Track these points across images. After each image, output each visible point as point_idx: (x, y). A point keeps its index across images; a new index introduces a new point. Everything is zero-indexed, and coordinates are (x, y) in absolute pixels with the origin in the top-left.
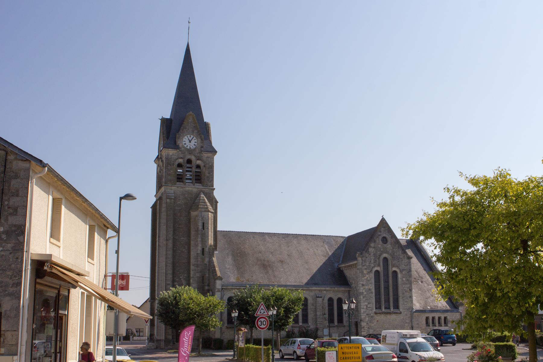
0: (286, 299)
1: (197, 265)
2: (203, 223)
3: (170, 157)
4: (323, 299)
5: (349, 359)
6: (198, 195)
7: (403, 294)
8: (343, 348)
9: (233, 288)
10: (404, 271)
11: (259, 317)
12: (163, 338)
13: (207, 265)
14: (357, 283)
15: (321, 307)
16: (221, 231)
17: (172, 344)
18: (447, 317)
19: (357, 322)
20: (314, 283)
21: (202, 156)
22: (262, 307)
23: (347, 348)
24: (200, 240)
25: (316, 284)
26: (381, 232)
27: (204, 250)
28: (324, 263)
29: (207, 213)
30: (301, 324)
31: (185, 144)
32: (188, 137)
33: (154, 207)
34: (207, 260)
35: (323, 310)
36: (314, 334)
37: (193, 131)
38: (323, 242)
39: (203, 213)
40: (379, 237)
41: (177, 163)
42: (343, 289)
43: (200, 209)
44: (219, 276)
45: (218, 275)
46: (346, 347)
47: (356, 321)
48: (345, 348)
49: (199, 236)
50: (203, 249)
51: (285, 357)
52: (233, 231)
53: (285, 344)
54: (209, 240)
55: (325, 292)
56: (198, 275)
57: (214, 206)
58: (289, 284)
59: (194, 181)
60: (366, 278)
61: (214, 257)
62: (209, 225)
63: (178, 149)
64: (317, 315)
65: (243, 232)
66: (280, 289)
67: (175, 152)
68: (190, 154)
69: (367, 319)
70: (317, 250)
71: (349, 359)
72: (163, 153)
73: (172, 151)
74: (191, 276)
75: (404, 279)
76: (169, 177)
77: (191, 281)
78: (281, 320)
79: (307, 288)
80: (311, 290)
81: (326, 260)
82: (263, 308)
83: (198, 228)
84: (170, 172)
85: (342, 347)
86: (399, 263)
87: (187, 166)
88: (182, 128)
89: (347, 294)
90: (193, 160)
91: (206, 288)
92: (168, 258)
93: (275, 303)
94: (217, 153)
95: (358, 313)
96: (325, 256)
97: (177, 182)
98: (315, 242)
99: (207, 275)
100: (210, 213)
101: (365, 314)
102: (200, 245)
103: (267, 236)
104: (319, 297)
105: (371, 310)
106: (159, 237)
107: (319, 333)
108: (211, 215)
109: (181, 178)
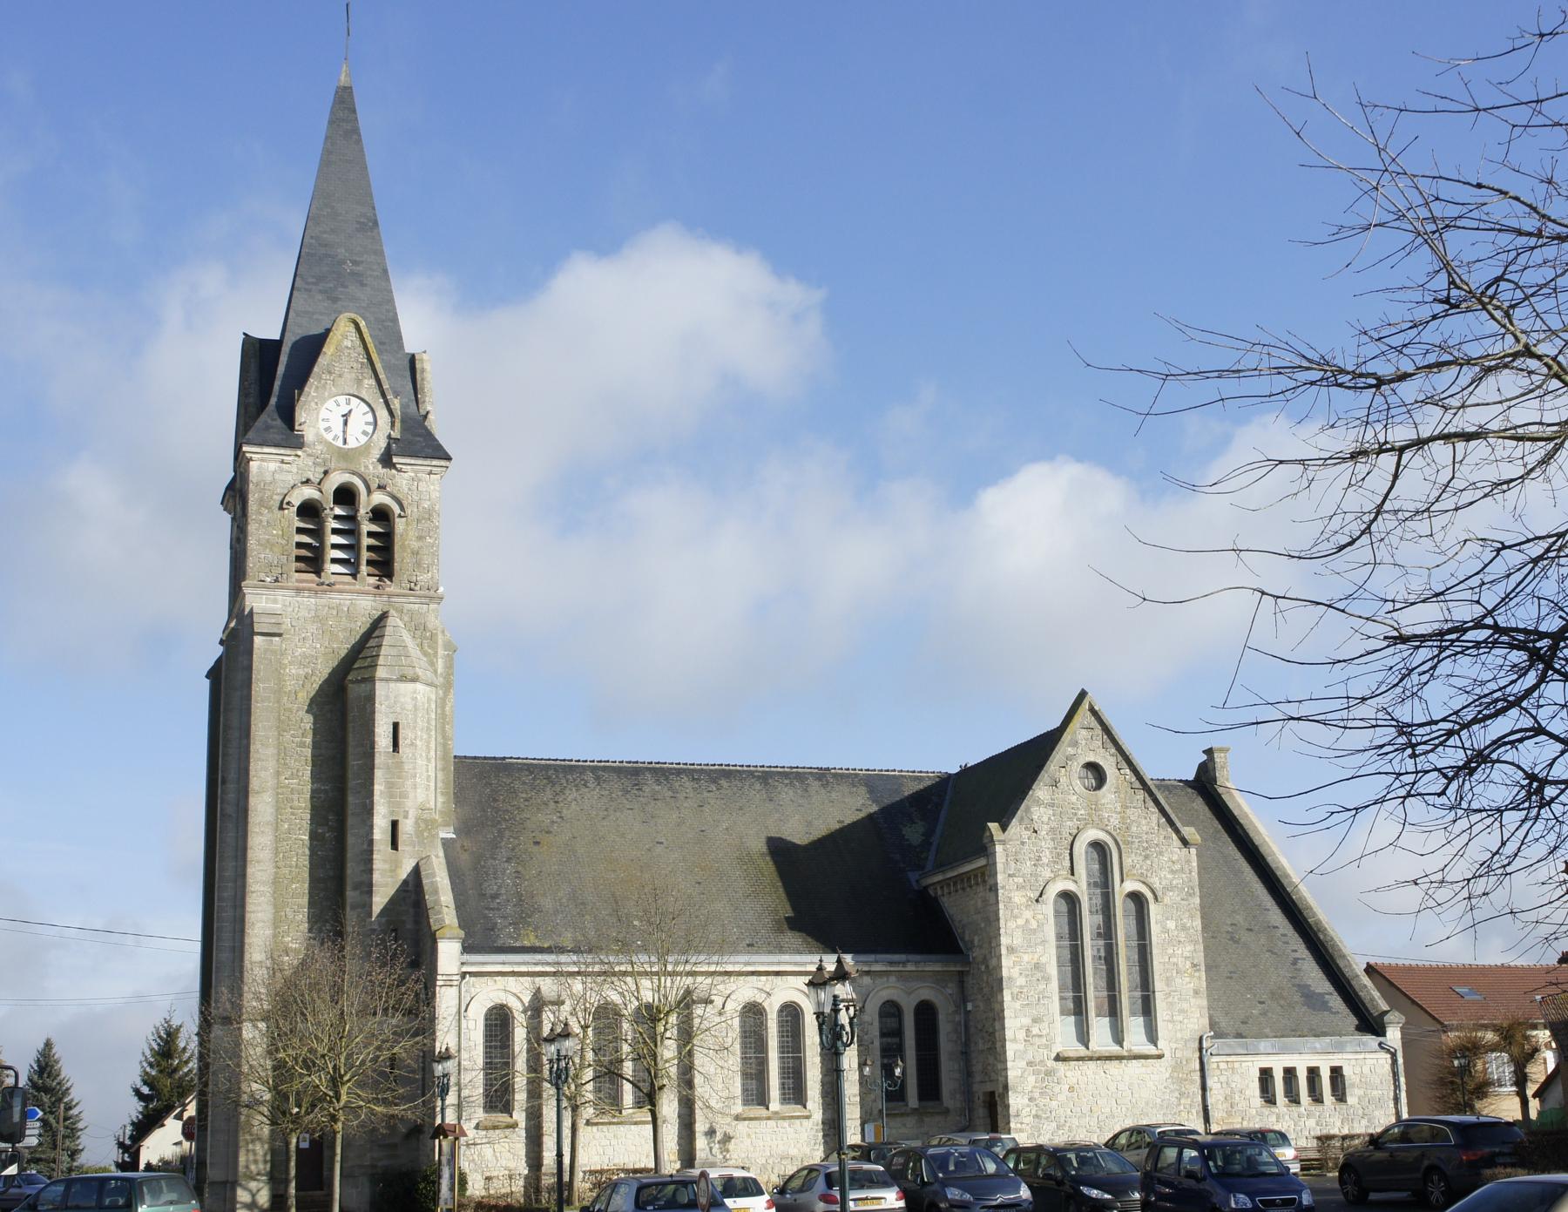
3: (269, 479)
7: (1168, 981)
10: (1171, 894)
14: (990, 943)
18: (1341, 1067)
19: (992, 1094)
24: (382, 788)
26: (1075, 744)
31: (328, 429)
40: (1069, 763)
42: (938, 967)
47: (992, 1090)
50: (395, 824)
57: (440, 660)
60: (1020, 922)
69: (1032, 1079)
75: (1171, 925)
86: (1149, 862)
89: (951, 989)
92: (258, 862)
95: (996, 1059)
101: (1023, 1064)
105: (1046, 1047)
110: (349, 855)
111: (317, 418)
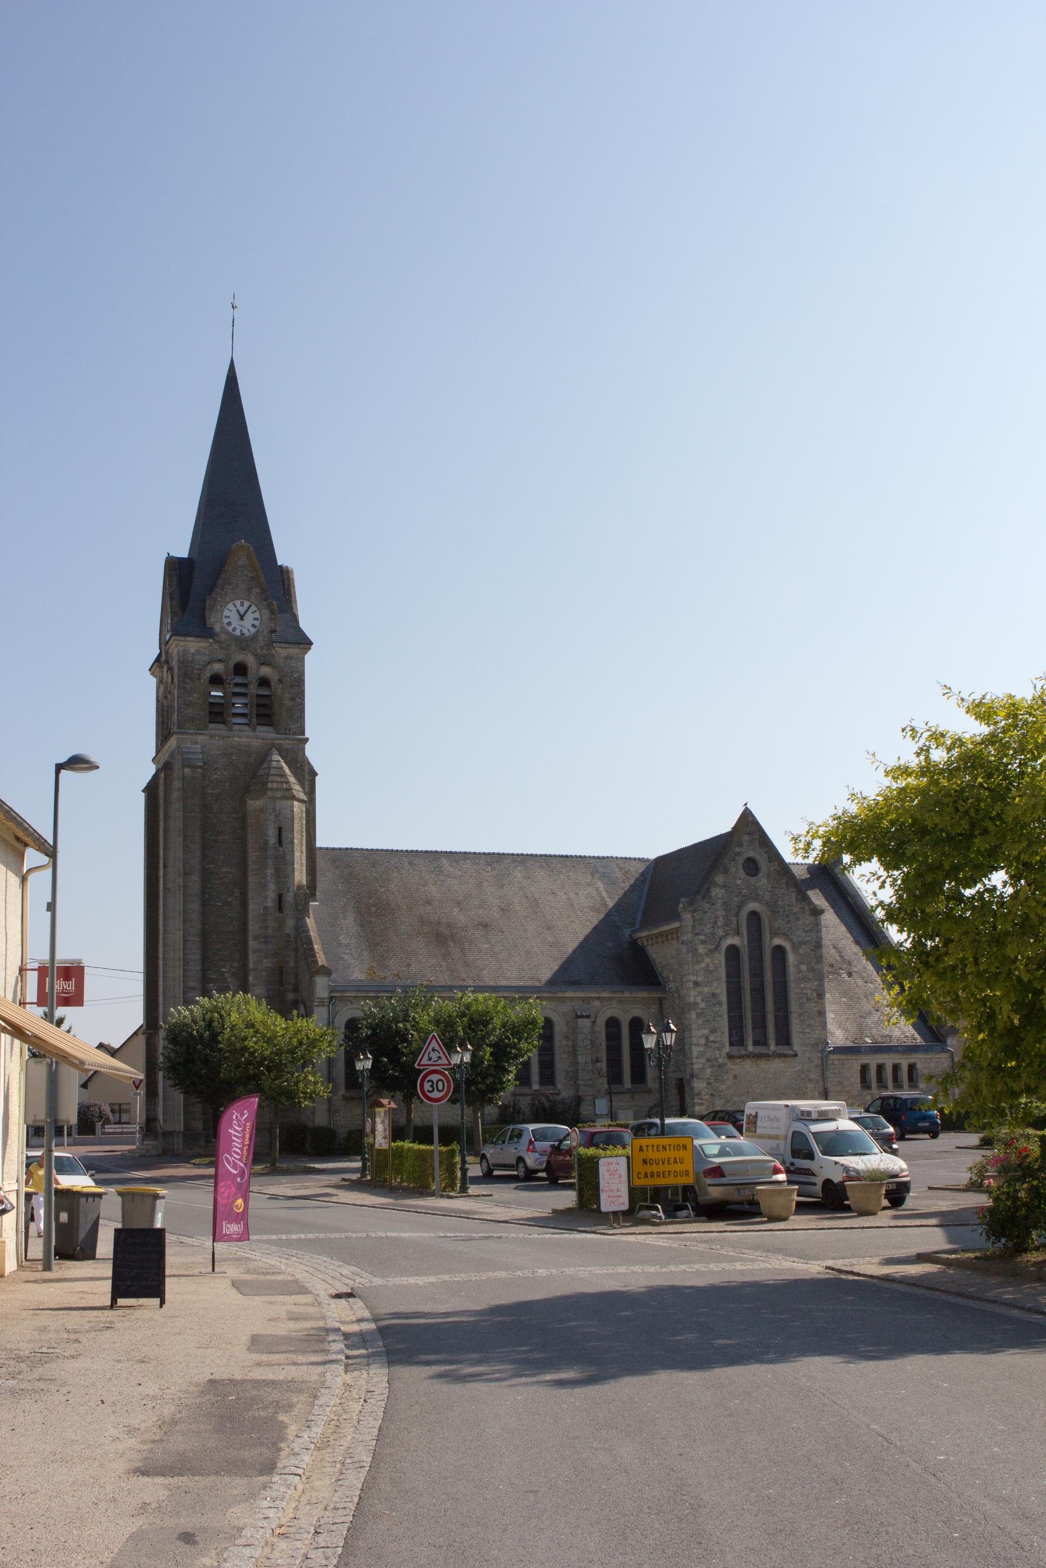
0: (497, 1022)
1: (266, 937)
2: (280, 830)
3: (190, 659)
4: (594, 1023)
5: (661, 1176)
6: (263, 757)
7: (801, 1005)
8: (645, 1149)
9: (360, 995)
10: (804, 947)
11: (426, 1069)
12: (180, 1127)
13: (292, 937)
14: (681, 979)
15: (587, 1042)
16: (327, 849)
17: (202, 1142)
18: (915, 1064)
19: (681, 1080)
20: (568, 982)
21: (274, 656)
22: (434, 1044)
23: (655, 1148)
24: (272, 871)
25: (575, 984)
26: (741, 845)
27: (283, 898)
28: (595, 928)
29: (289, 803)
30: (536, 1086)
31: (229, 624)
32: (235, 606)
33: (151, 790)
34: (290, 923)
35: (594, 1048)
36: (571, 1112)
37: (249, 590)
38: (592, 875)
39: (278, 802)
40: (737, 858)
41: (208, 674)
42: (645, 995)
43: (269, 793)
44: (323, 966)
45: (320, 964)
46: (653, 1146)
47: (681, 1076)
48: (650, 1148)
49: (270, 862)
50: (280, 896)
51: (496, 1173)
52: (357, 849)
53: (494, 1140)
54: (296, 873)
55: (597, 1003)
56: (267, 963)
57: (307, 783)
58: (504, 983)
59: (254, 720)
60: (703, 965)
61: (309, 917)
62: (296, 834)
63: (210, 638)
64: (578, 1063)
65: (382, 850)
66: (481, 996)
67: (203, 645)
68: (242, 649)
69: (709, 1071)
70: (577, 894)
71: (661, 1176)
72: (172, 648)
73: (196, 644)
74: (251, 966)
75: (804, 968)
76: (189, 711)
77: (251, 979)
78: (485, 1077)
79: (551, 992)
80: (562, 1000)
81: (601, 921)
82: (437, 1047)
83: (266, 843)
84: (191, 699)
85: (641, 1147)
86: (789, 925)
87: (235, 681)
88: (220, 582)
89: (654, 1009)
90: (249, 665)
91: (291, 996)
92: (190, 921)
93: (468, 1034)
94: (312, 647)
95: (684, 1056)
96: (598, 911)
97: (210, 722)
98: (571, 874)
99: (292, 964)
100: (296, 803)
101: (703, 1060)
102: (272, 886)
103: (445, 861)
104: (582, 1017)
105: (719, 1049)
106: (165, 867)
107: (585, 1110)
108: (298, 808)
109: (221, 714)
110: (251, 915)
111: (222, 615)
